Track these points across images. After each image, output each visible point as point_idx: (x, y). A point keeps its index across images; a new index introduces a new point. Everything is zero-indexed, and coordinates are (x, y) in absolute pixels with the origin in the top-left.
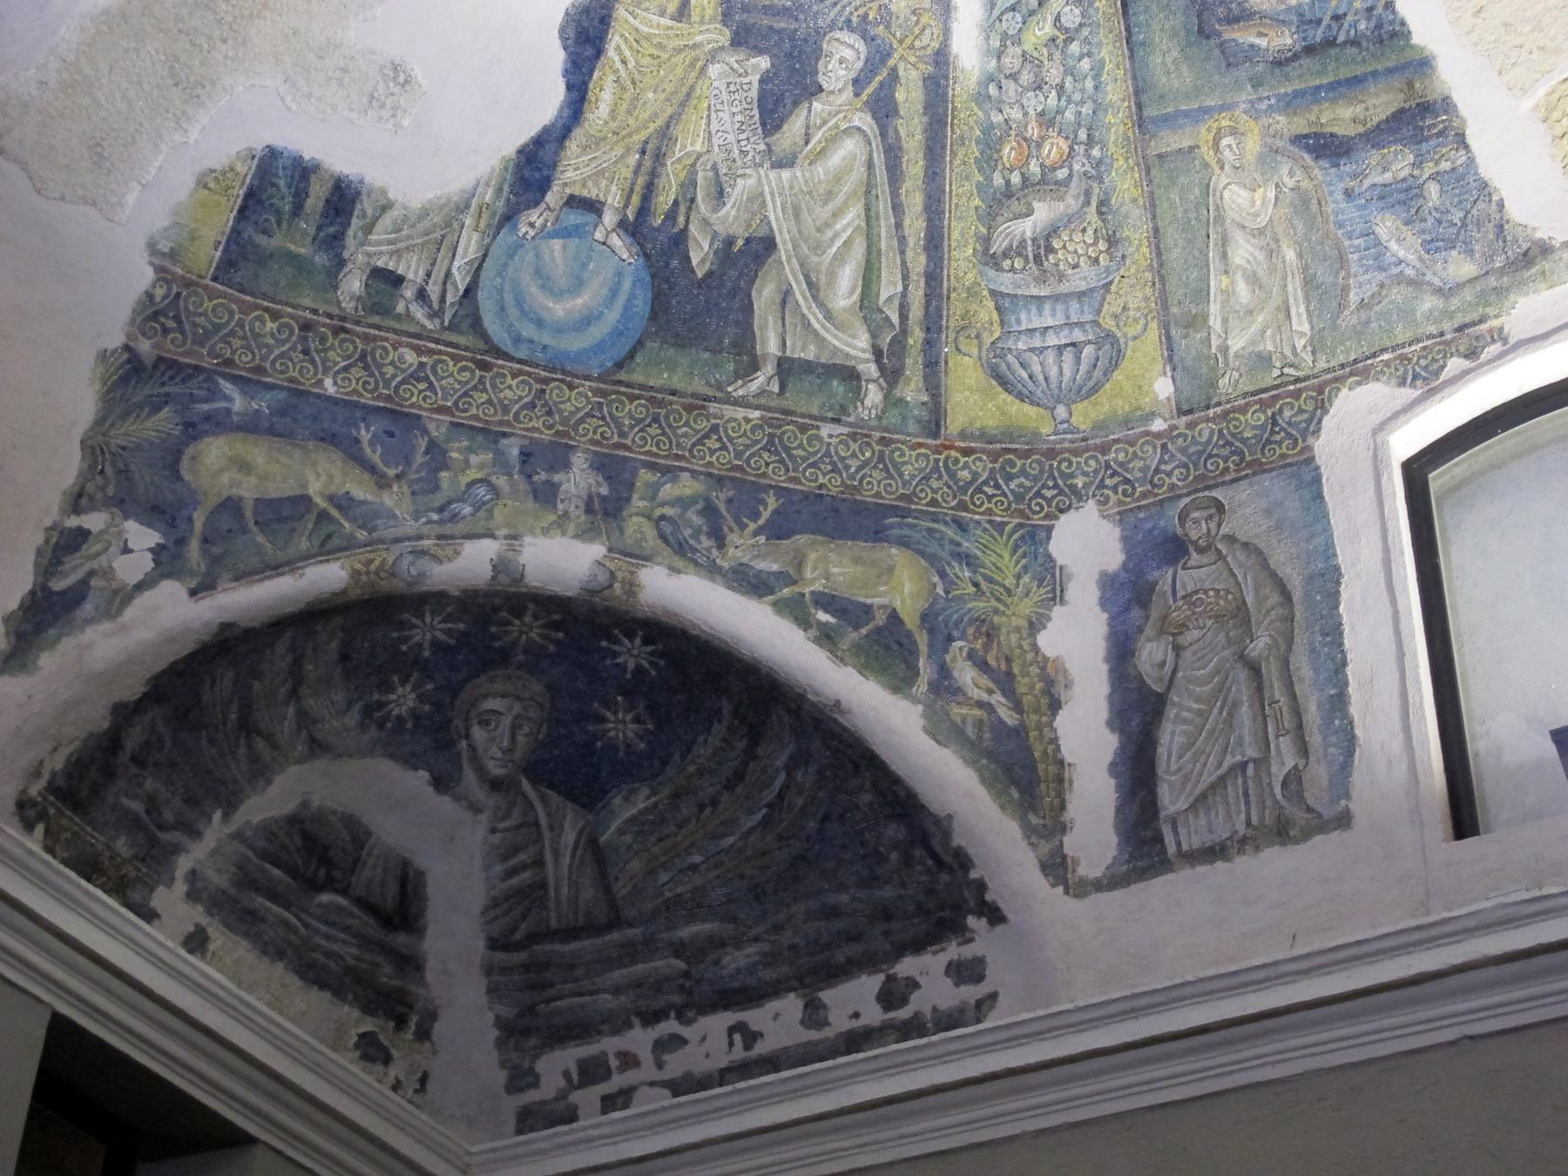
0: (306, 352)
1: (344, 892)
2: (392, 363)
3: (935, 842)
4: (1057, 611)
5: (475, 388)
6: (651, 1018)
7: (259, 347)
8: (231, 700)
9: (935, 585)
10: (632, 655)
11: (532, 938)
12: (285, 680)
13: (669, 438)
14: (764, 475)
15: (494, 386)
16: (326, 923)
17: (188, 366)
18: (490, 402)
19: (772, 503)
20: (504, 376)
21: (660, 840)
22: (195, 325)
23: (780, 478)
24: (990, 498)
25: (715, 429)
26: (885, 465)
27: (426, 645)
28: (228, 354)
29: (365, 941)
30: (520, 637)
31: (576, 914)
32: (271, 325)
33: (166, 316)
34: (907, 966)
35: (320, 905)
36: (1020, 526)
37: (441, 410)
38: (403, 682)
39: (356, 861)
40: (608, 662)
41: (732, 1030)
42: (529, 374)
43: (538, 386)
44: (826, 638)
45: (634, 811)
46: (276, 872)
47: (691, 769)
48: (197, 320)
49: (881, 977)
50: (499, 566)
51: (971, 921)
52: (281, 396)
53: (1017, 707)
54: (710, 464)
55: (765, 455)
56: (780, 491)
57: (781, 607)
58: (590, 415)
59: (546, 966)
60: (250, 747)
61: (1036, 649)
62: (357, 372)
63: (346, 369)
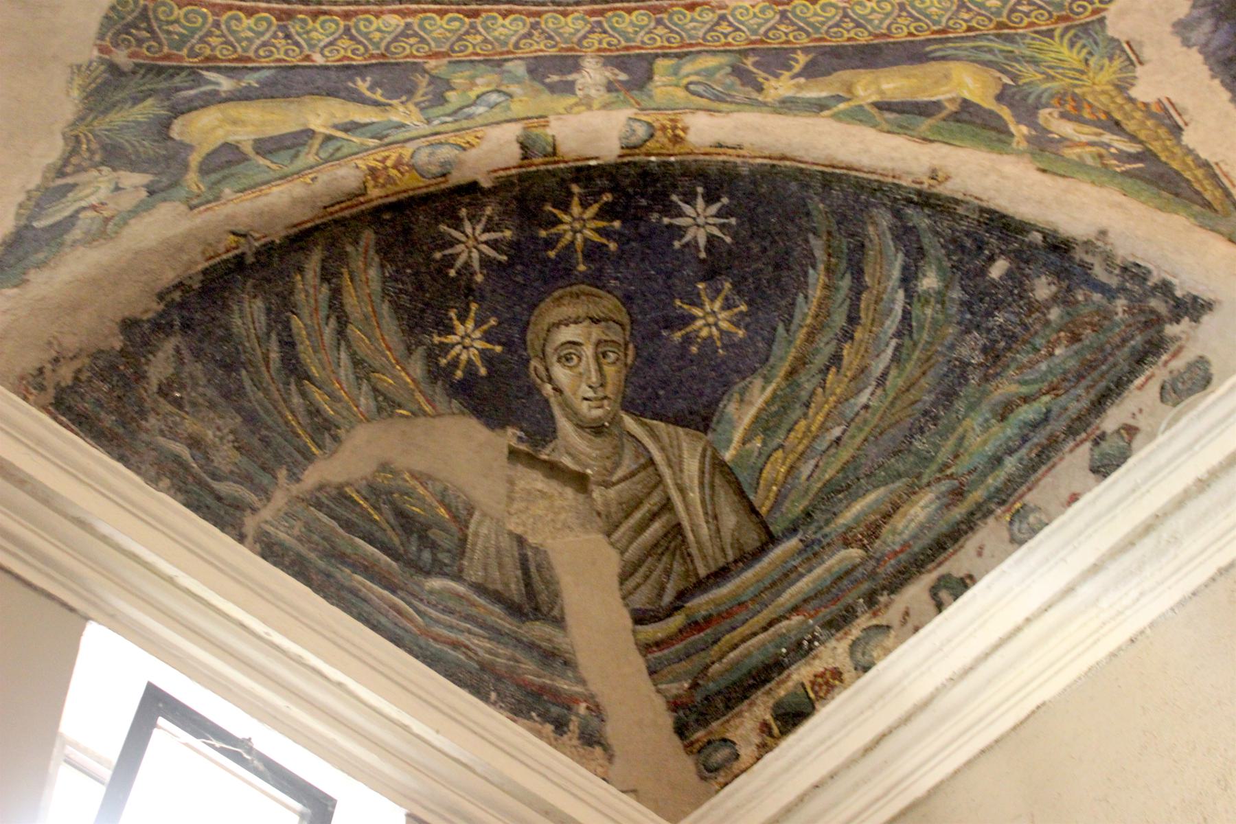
0: (288, 36)
1: (458, 577)
2: (379, 30)
3: (1099, 272)
4: (1139, 70)
5: (467, 33)
6: (837, 624)
7: (239, 41)
8: (268, 334)
9: (1000, 78)
10: (699, 222)
11: (682, 596)
12: (328, 318)
13: (678, 33)
14: (788, 42)
15: (486, 28)
16: (443, 611)
17: (170, 67)
18: (485, 41)
19: (802, 59)
20: (495, 18)
21: (790, 431)
22: (169, 33)
23: (804, 41)
24: (1027, 15)
25: (723, 18)
26: (908, 12)
27: (476, 265)
28: (208, 52)
29: (496, 634)
30: (574, 238)
31: (723, 550)
32: (248, 22)
33: (137, 28)
34: (1112, 420)
35: (431, 592)
36: (1067, 29)
37: (436, 55)
38: (463, 318)
39: (464, 540)
40: (677, 244)
41: (934, 592)
42: (520, 12)
43: (532, 20)
44: (901, 129)
45: (753, 411)
46: (370, 549)
47: (802, 334)
48: (171, 28)
49: (1088, 445)
50: (525, 147)
51: (1171, 330)
52: (266, 73)
53: (1133, 138)
54: (729, 44)
55: (783, 28)
56: (806, 50)
57: (837, 117)
58: (592, 31)
59: (708, 620)
60: (303, 394)
61: (1131, 100)
62: (345, 42)
63: (331, 43)
